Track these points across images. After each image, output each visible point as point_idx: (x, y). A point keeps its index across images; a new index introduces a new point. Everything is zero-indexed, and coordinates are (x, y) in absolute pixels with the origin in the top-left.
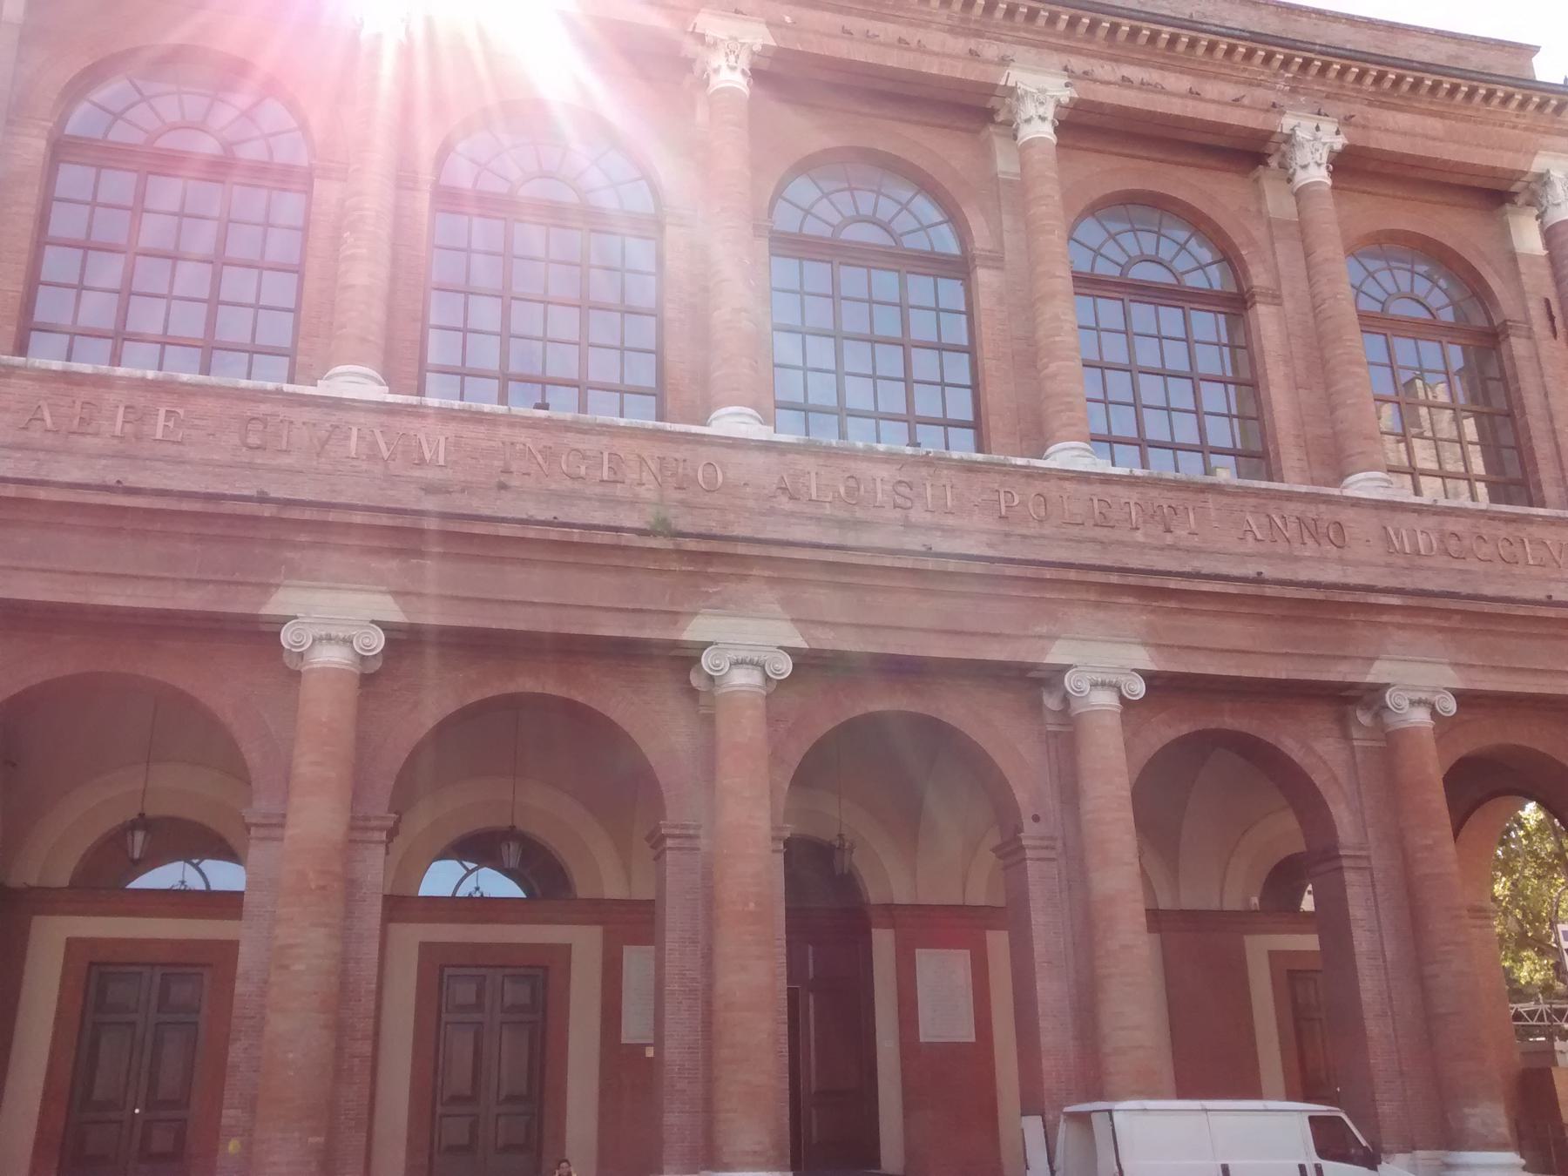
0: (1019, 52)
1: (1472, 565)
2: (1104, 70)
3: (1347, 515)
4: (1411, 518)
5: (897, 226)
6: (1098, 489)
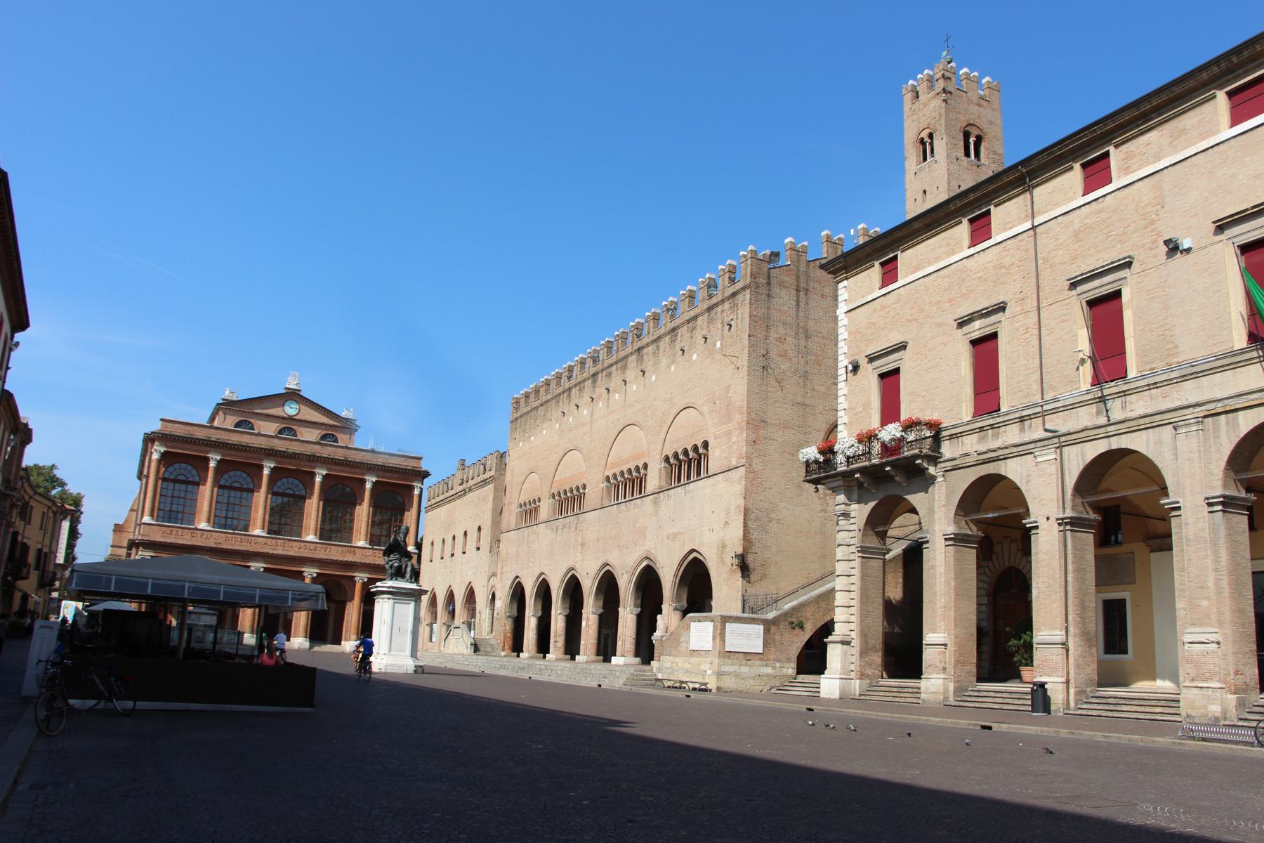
0: (319, 464)
1: (377, 558)
2: (333, 467)
3: (356, 549)
4: (368, 550)
5: (295, 490)
6: (316, 545)
